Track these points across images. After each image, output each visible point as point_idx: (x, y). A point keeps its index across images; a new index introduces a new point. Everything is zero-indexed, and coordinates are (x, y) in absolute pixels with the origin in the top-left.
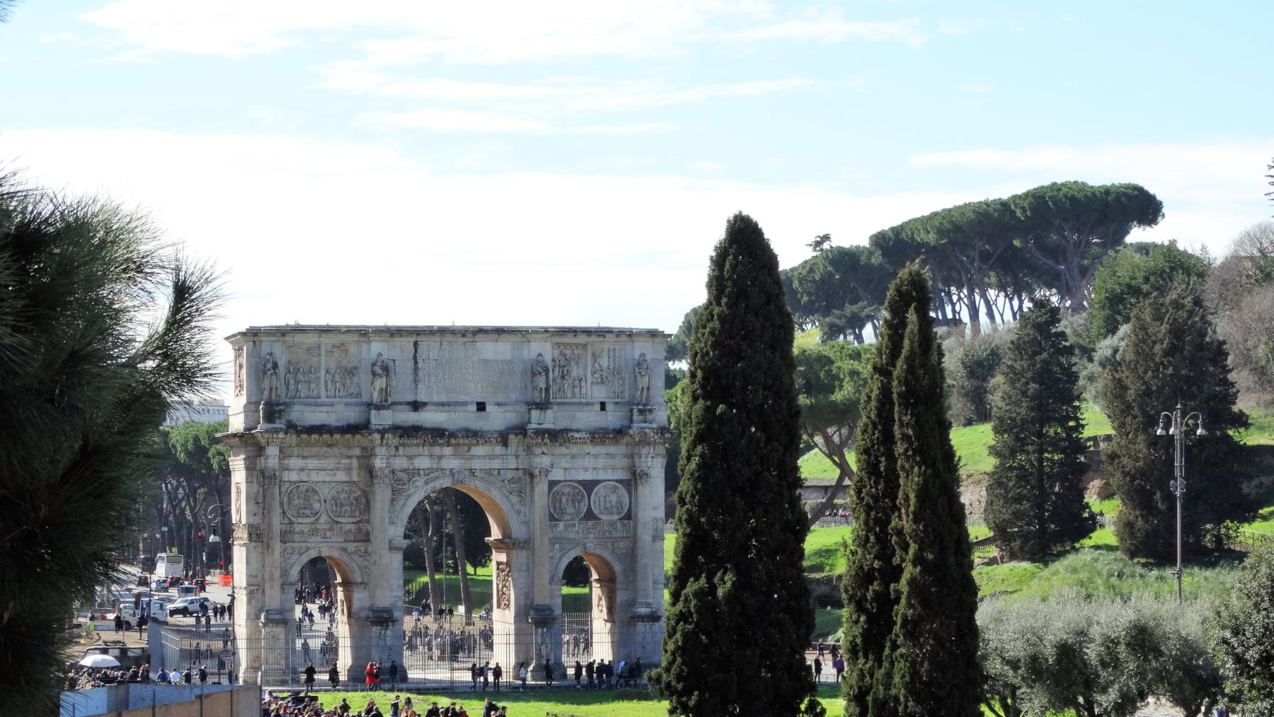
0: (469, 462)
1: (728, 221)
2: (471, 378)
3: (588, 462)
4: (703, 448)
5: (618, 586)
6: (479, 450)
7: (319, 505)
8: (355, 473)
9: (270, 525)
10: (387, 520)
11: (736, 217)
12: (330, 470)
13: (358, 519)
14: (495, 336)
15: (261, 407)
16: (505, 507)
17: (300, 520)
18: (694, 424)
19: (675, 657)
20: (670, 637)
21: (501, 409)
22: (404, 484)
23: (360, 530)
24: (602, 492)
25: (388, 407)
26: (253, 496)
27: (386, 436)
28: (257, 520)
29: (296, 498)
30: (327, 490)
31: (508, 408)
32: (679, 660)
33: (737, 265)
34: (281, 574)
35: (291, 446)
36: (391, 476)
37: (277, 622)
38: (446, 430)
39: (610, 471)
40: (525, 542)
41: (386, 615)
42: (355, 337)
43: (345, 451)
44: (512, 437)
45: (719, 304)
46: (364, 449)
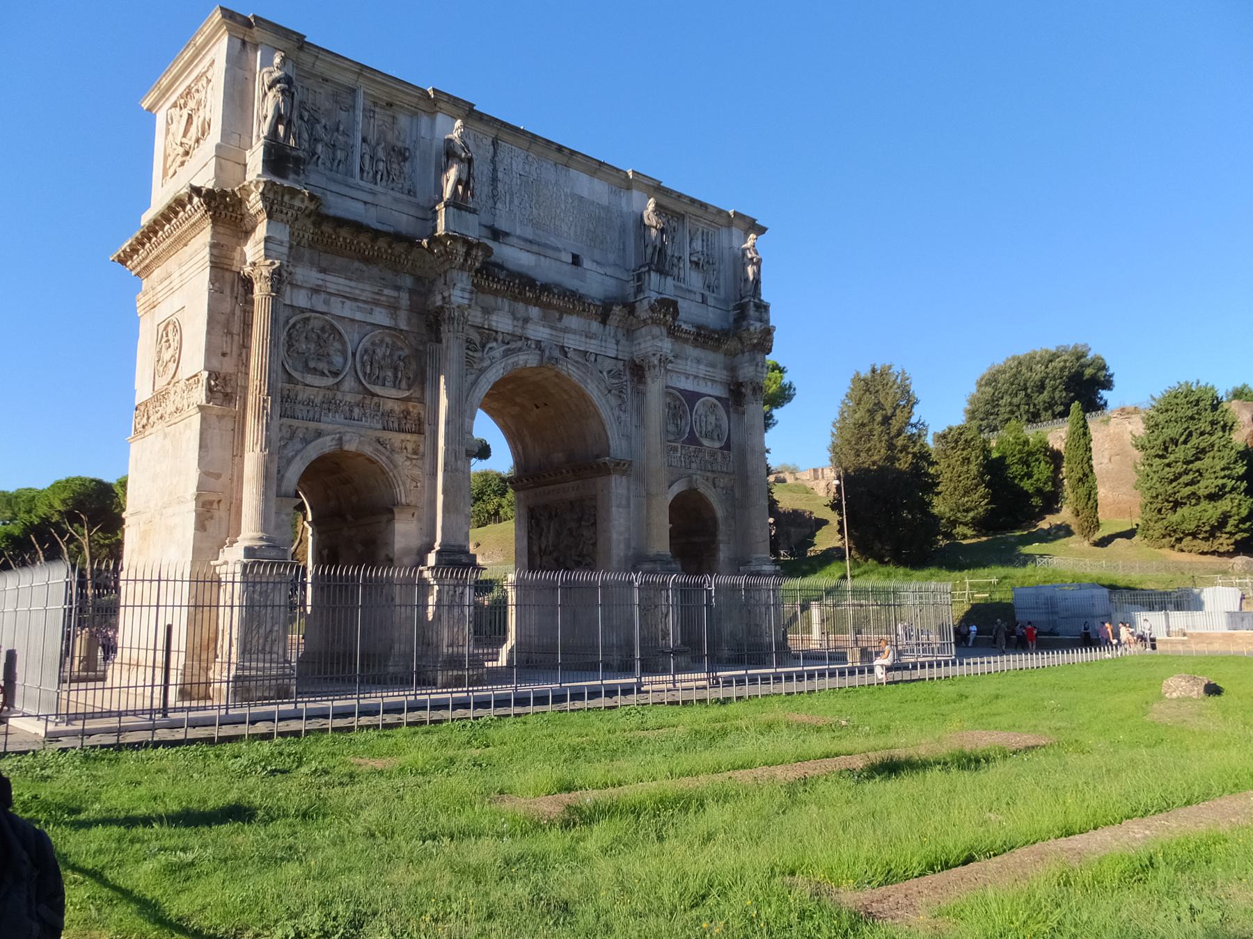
0: (561, 334)
3: (690, 367)
5: (721, 537)
6: (573, 321)
8: (403, 315)
12: (365, 302)
13: (406, 394)
16: (605, 412)
17: (310, 379)
22: (476, 351)
23: (406, 414)
24: (701, 411)
26: (222, 318)
29: (302, 338)
30: (356, 337)
39: (709, 384)
40: (630, 463)
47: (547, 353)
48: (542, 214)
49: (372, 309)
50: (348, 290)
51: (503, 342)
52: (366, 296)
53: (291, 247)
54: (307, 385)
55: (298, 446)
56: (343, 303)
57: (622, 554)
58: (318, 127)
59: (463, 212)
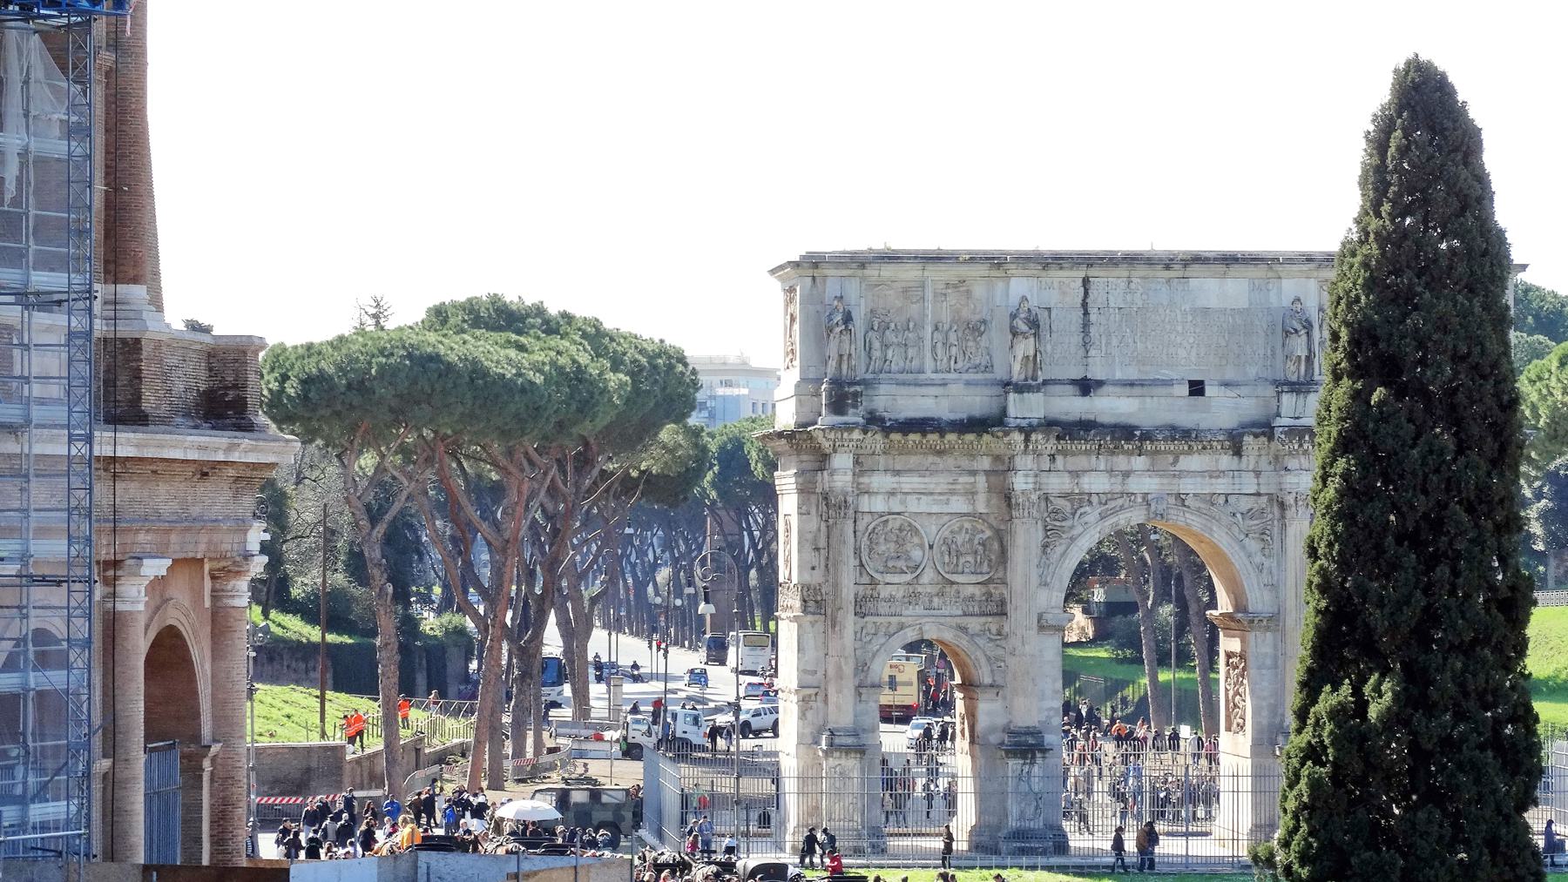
0: (1175, 481)
1: (1396, 71)
2: (1179, 339)
4: (1348, 462)
7: (921, 553)
9: (836, 586)
10: (1035, 580)
11: (1408, 63)
12: (940, 494)
13: (987, 577)
14: (1221, 268)
15: (823, 387)
17: (889, 578)
18: (1333, 420)
19: (1298, 821)
20: (1291, 786)
21: (1230, 393)
25: (1038, 389)
26: (809, 536)
27: (1033, 437)
28: (817, 577)
30: (934, 529)
31: (1244, 390)
32: (1304, 827)
33: (1408, 148)
34: (856, 669)
35: (873, 454)
36: (1043, 504)
37: (847, 750)
38: (1137, 428)
40: (1270, 619)
41: (1031, 741)
42: (982, 270)
43: (965, 463)
44: (1248, 439)
45: (1378, 215)
46: (997, 458)
47: (1153, 508)
48: (1149, 347)
49: (948, 499)
50: (923, 486)
51: (1100, 503)
52: (943, 488)
53: (854, 475)
54: (888, 584)
55: (883, 640)
56: (919, 499)
57: (1265, 722)
58: (887, 332)
59: (1026, 395)
